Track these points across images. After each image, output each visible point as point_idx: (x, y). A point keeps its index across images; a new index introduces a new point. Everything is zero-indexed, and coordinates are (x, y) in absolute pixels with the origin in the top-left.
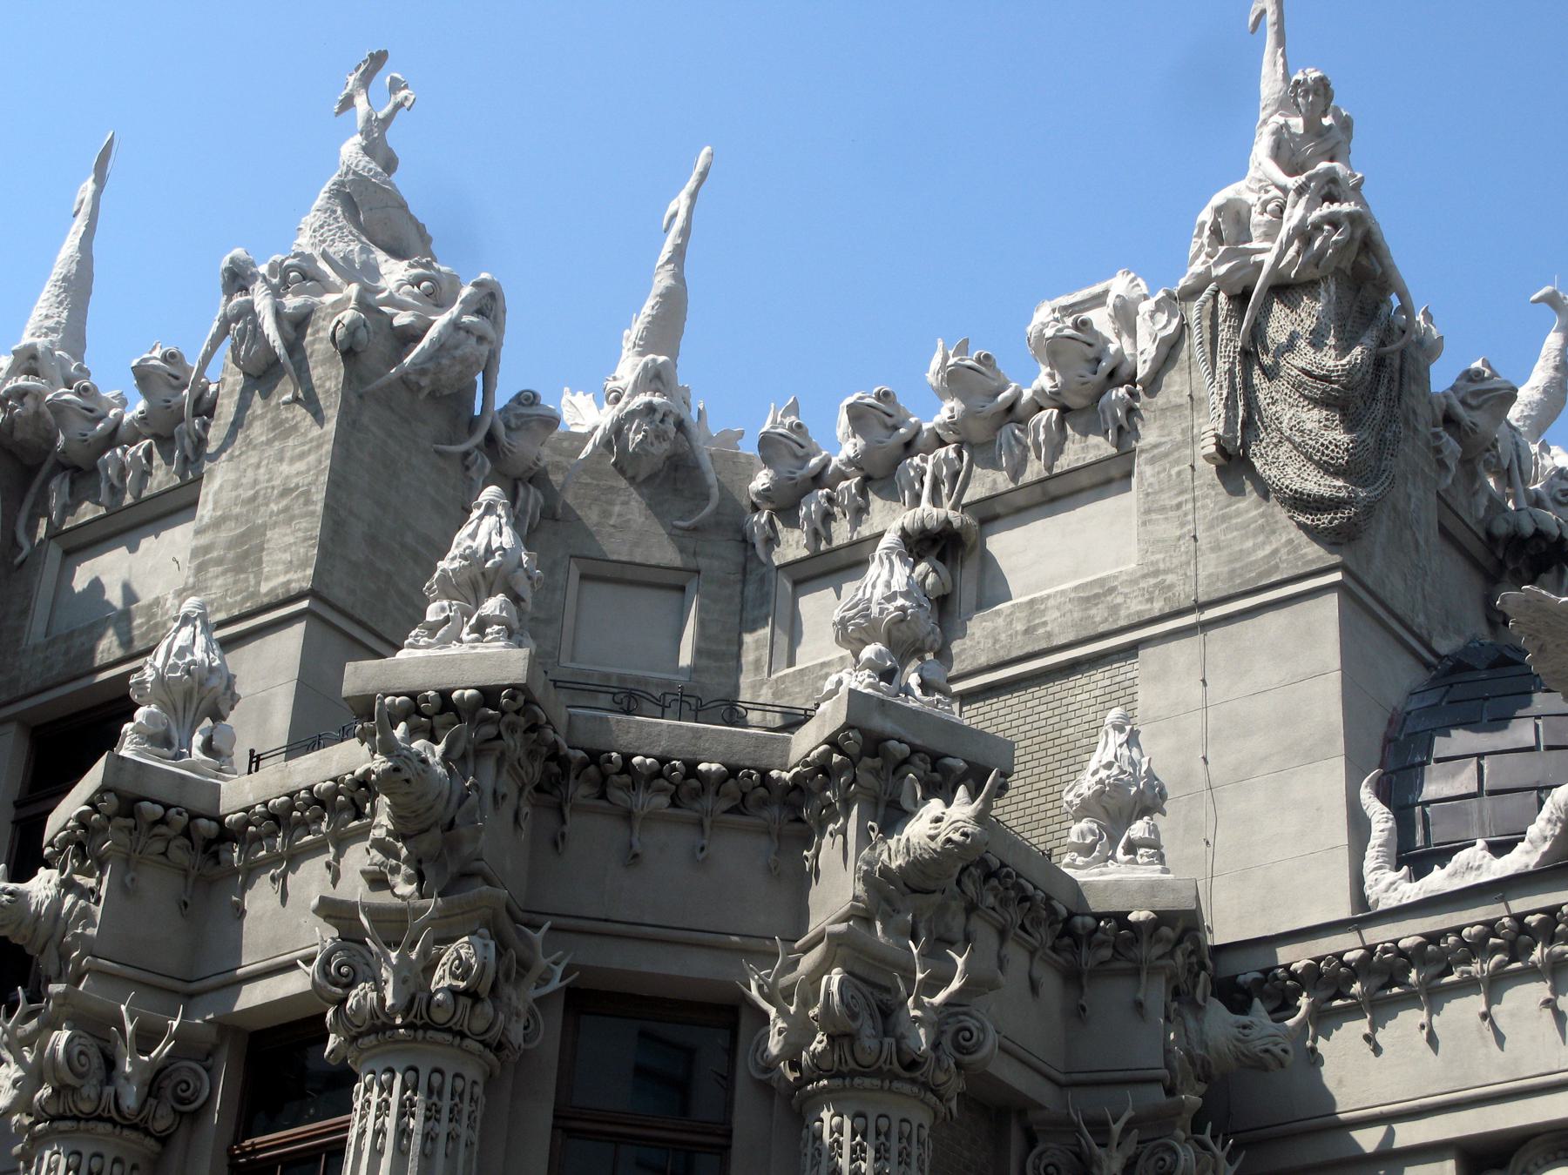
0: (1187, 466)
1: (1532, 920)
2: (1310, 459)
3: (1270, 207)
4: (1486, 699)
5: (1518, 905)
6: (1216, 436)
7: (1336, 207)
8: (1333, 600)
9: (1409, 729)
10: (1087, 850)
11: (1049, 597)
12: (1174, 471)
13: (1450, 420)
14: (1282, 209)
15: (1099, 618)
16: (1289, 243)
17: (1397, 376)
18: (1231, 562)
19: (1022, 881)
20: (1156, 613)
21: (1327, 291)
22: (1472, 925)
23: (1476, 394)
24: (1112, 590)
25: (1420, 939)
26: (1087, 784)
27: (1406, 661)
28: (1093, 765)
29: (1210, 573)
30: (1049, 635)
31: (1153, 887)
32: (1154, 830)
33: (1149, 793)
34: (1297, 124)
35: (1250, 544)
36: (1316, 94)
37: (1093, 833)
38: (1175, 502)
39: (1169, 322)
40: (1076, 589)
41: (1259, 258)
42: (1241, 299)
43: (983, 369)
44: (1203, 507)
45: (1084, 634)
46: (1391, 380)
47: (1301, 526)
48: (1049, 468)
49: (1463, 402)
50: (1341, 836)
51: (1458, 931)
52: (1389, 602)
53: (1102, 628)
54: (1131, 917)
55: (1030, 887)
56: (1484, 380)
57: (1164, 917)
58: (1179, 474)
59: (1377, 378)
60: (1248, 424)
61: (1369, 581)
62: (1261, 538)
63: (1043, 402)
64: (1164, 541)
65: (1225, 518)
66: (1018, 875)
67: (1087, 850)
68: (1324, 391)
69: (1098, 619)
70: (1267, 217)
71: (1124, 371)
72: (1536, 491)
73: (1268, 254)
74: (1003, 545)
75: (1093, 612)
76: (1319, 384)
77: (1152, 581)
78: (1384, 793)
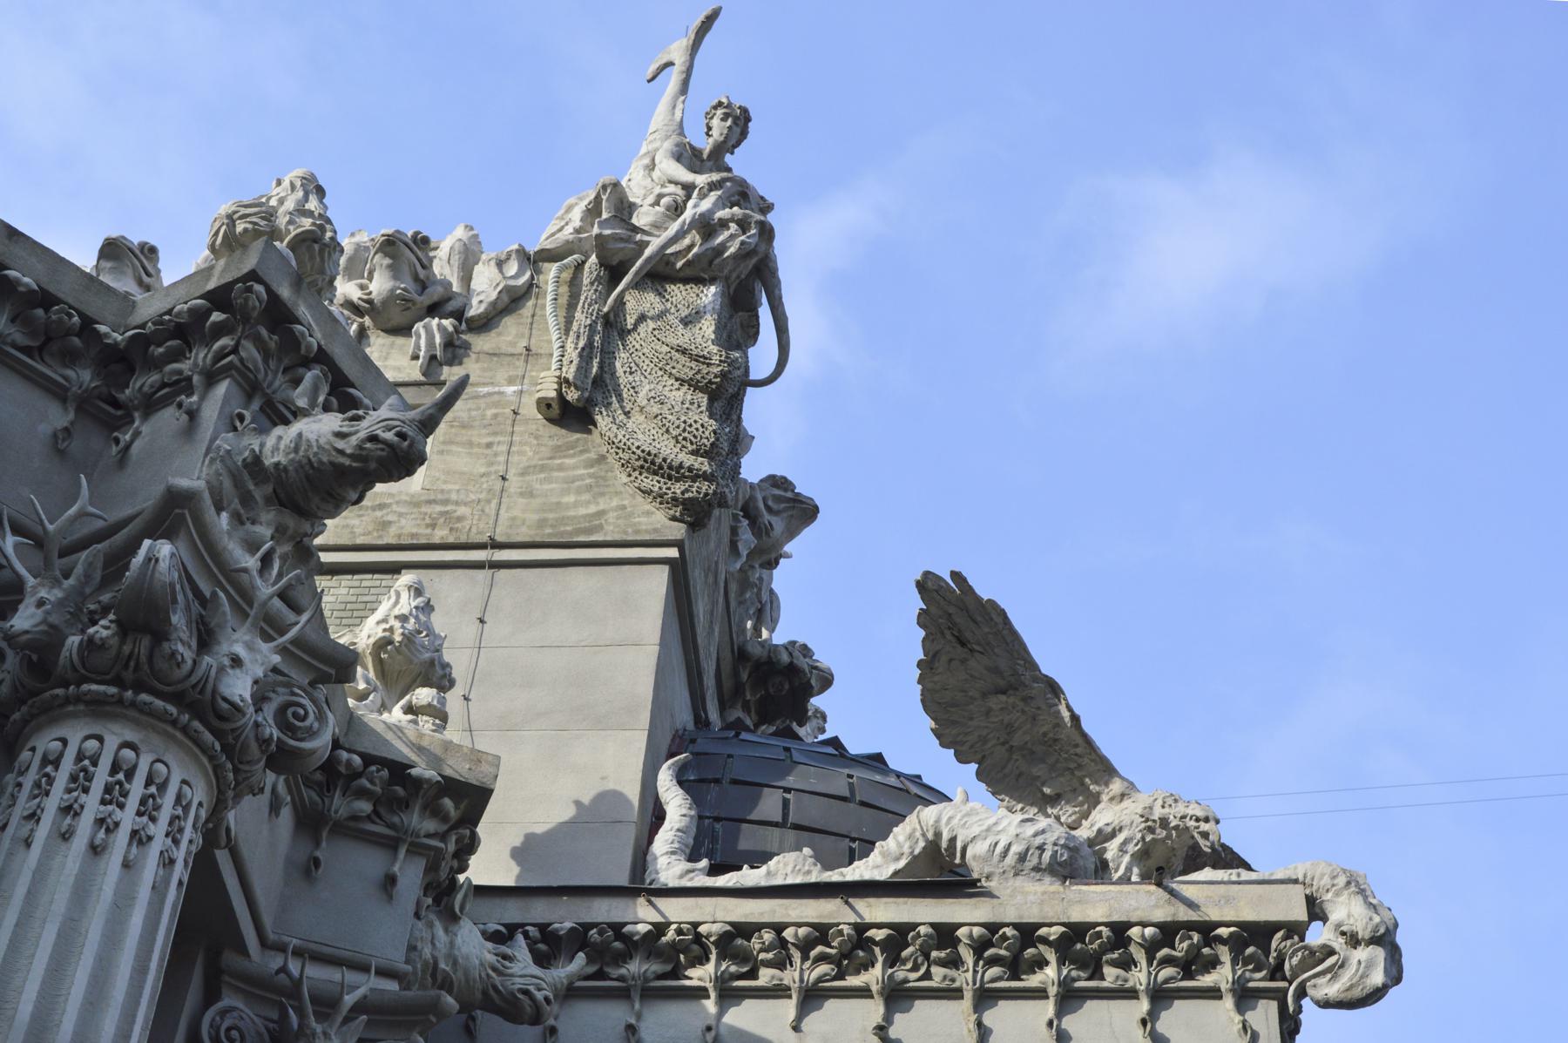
0: (508, 411)
12: (489, 413)
13: (749, 511)
20: (436, 540)
22: (799, 925)
23: (778, 499)
25: (728, 928)
35: (571, 499)
38: (485, 440)
41: (646, 238)
42: (613, 272)
44: (519, 453)
51: (778, 928)
58: (495, 416)
62: (585, 497)
65: (543, 468)
77: (439, 508)
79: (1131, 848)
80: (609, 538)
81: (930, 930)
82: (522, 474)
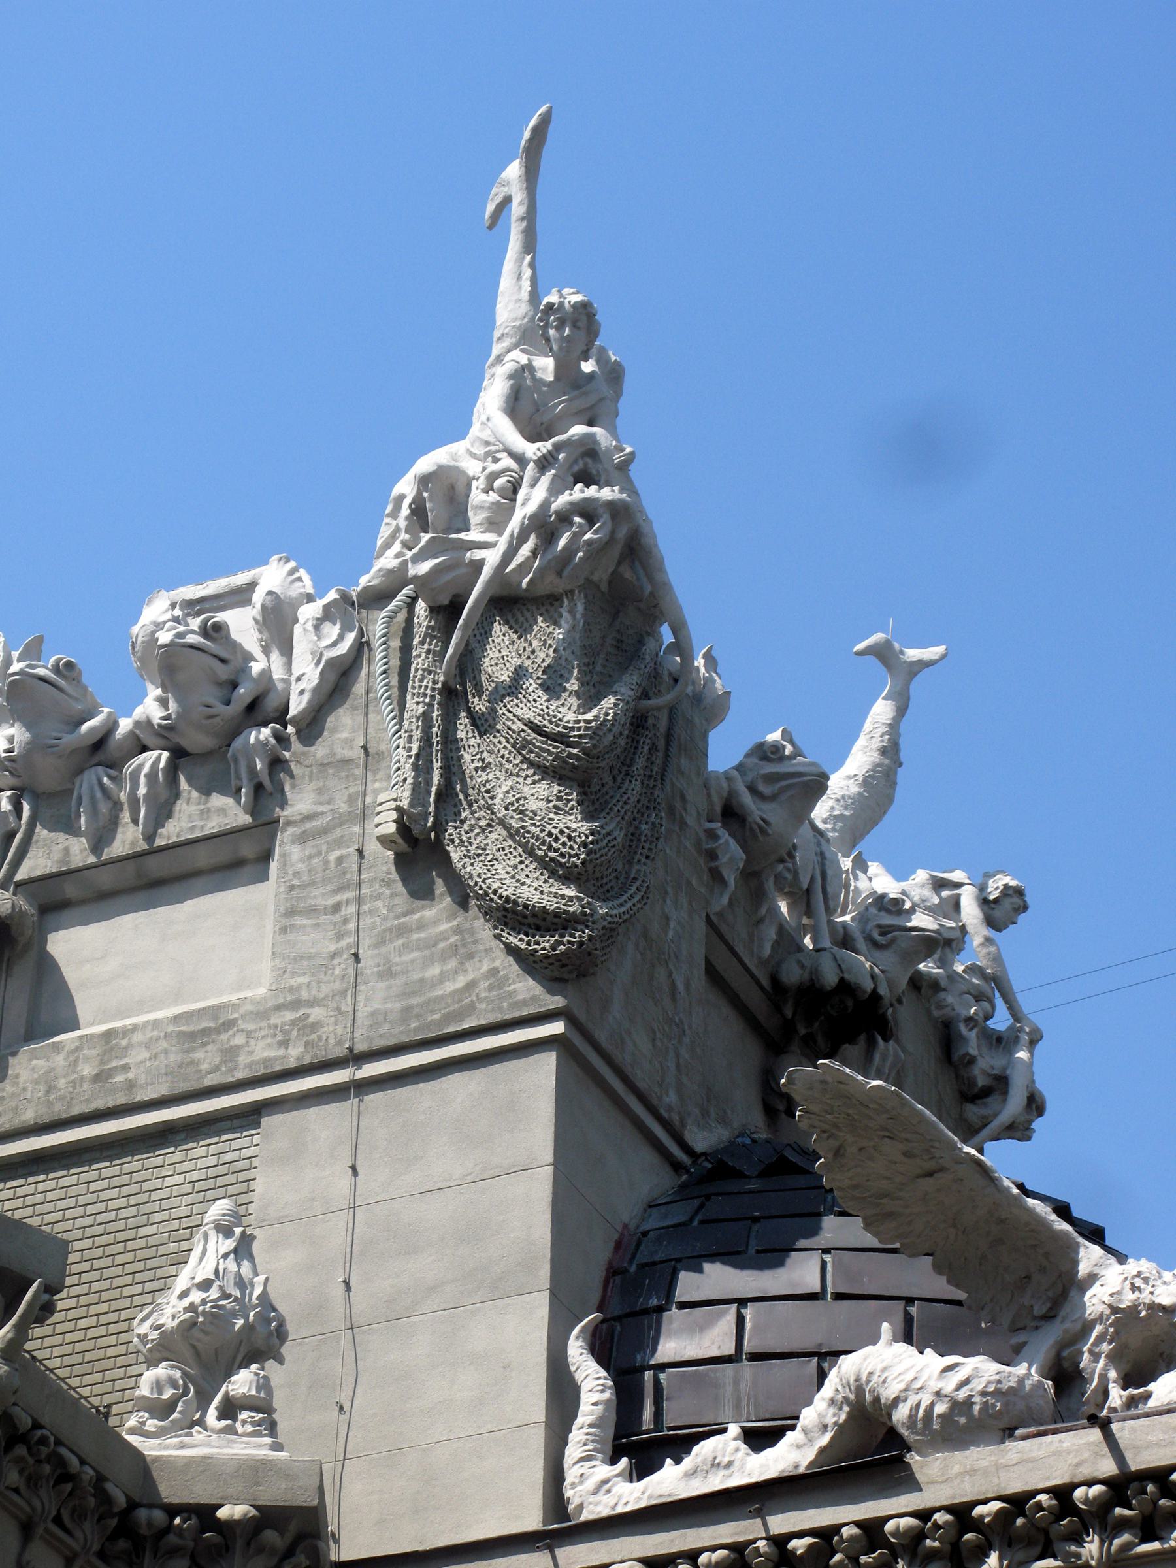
0: (352, 850)
1: (799, 1545)
2: (531, 853)
3: (499, 482)
4: (756, 1220)
5: (780, 1523)
6: (398, 809)
7: (592, 491)
8: (548, 1061)
9: (641, 1258)
10: (163, 1410)
11: (135, 1028)
12: (332, 857)
14: (515, 487)
15: (208, 1064)
16: (522, 538)
17: (661, 743)
18: (406, 995)
19: (63, 1451)
20: (292, 1063)
21: (572, 612)
22: (713, 1549)
23: (771, 778)
24: (229, 1025)
26: (171, 1311)
27: (648, 1156)
28: (182, 1283)
29: (376, 1009)
30: (131, 1085)
31: (256, 1470)
32: (264, 1384)
33: (261, 1329)
34: (546, 366)
35: (434, 971)
36: (574, 326)
37: (173, 1383)
38: (330, 902)
39: (341, 637)
40: (176, 1019)
41: (478, 555)
43: (62, 682)
44: (371, 912)
45: (183, 1087)
46: (654, 748)
47: (511, 950)
48: (150, 837)
49: (752, 789)
50: (535, 1407)
52: (628, 1070)
53: (210, 1081)
54: (222, 1513)
55: (75, 1461)
56: (782, 758)
57: (269, 1517)
58: (340, 860)
59: (634, 743)
60: (446, 795)
61: (602, 1037)
62: (452, 964)
63: (148, 740)
64: (310, 958)
65: (402, 931)
66: (58, 1442)
67: (163, 1410)
68: (557, 757)
69: (205, 1067)
70: (493, 497)
71: (271, 703)
72: (844, 924)
73: (491, 551)
74: (75, 947)
75: (199, 1055)
76: (551, 746)
77: (289, 1016)
78: (601, 1350)
79: (1105, 1347)
80: (483, 1022)
81: (855, 1531)
82: (377, 945)
